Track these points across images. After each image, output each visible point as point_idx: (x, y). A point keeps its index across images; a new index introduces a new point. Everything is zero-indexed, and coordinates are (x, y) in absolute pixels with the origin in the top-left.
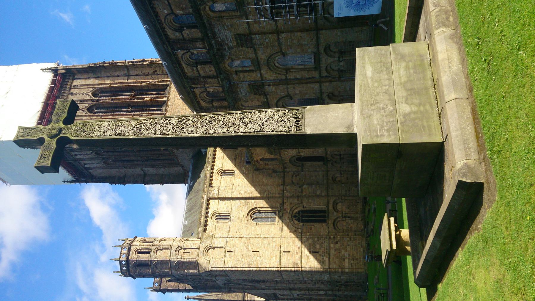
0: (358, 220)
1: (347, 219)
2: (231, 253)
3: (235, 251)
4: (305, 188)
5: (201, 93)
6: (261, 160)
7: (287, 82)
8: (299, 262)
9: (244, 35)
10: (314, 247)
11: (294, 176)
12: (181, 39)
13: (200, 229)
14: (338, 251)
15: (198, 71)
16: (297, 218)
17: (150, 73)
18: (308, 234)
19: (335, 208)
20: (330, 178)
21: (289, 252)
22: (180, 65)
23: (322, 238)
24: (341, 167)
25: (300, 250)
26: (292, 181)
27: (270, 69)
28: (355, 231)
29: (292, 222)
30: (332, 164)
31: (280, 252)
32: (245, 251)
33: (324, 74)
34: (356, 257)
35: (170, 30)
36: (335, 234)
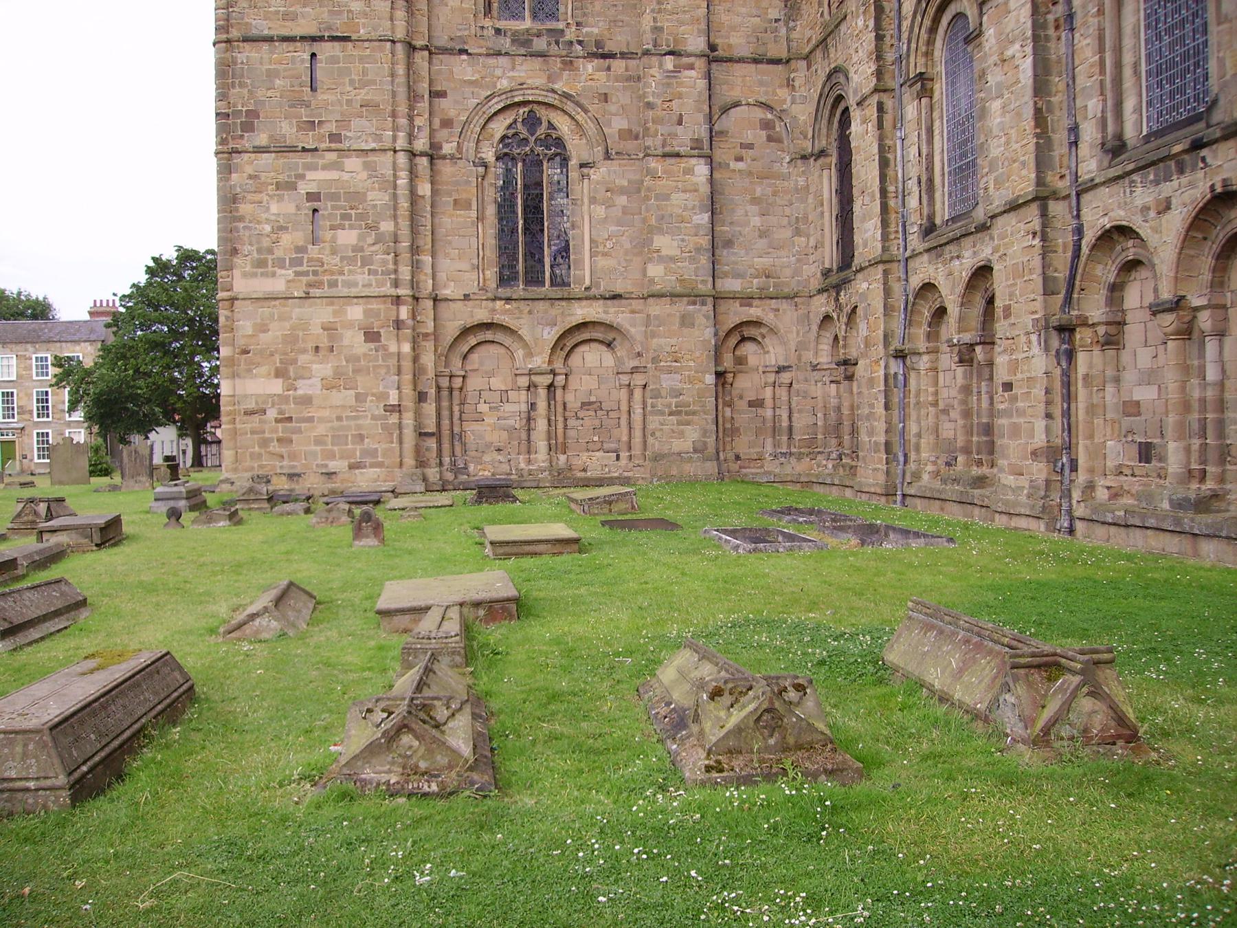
4: (689, 171)
8: (262, 139)
11: (769, 116)
16: (524, 133)
19: (586, 336)
20: (754, 312)
21: (313, 89)
23: (396, 263)
24: (815, 368)
25: (323, 146)
26: (737, 104)
28: (457, 437)
30: (827, 318)
31: (314, 39)
34: (294, 437)
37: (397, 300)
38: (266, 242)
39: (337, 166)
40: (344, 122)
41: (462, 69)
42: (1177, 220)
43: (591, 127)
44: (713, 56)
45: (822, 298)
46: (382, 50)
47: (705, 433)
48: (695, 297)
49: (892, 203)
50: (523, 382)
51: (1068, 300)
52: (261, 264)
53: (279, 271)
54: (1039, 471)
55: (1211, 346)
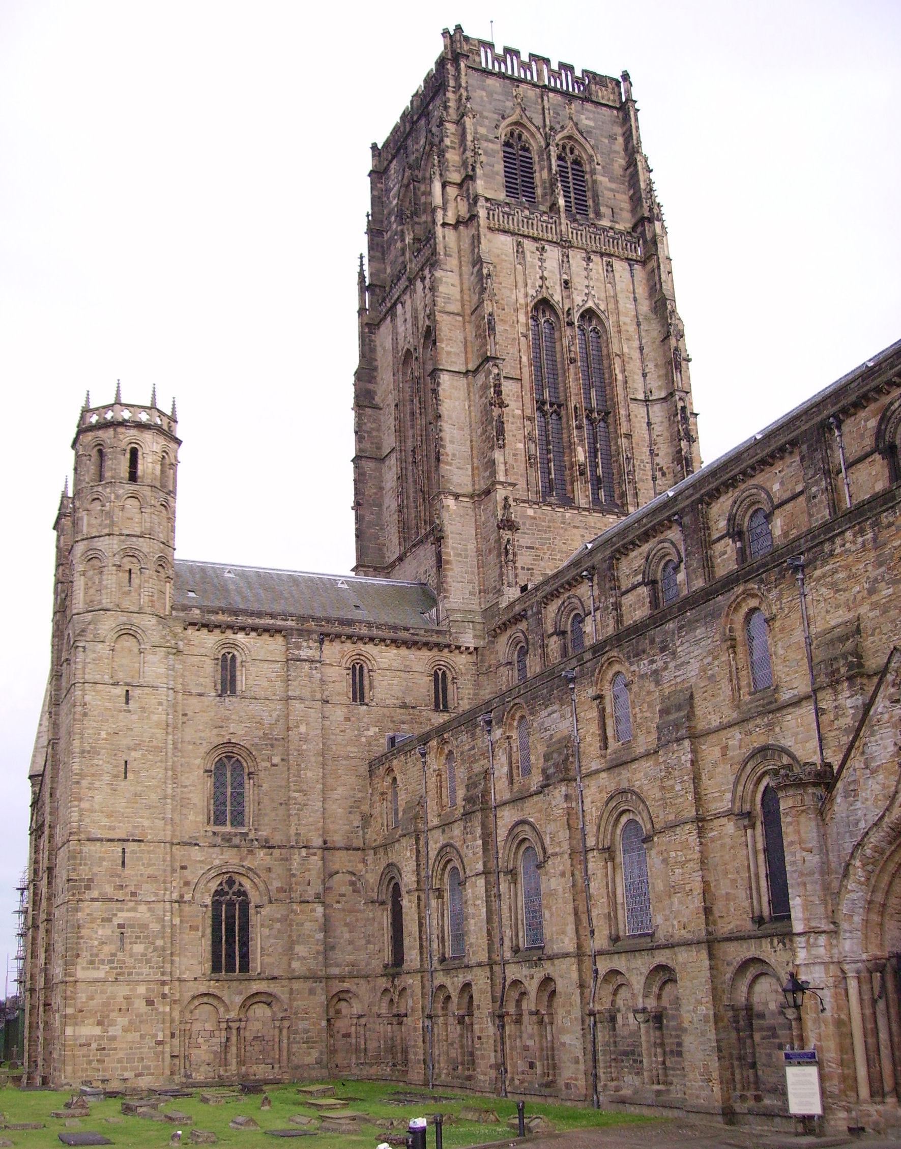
2: (124, 700)
3: (130, 711)
4: (313, 910)
5: (580, 600)
6: (395, 779)
7: (579, 854)
8: (95, 894)
9: (691, 716)
10: (138, 937)
12: (709, 535)
13: (197, 611)
14: (124, 1007)
15: (634, 587)
16: (226, 889)
17: (657, 460)
18: (177, 921)
19: (257, 999)
20: (346, 985)
22: (646, 536)
23: (163, 962)
24: (379, 1016)
25: (129, 898)
26: (337, 873)
27: (611, 798)
29: (213, 873)
30: (386, 990)
31: (124, 840)
32: (127, 742)
33: (604, 966)
35: (730, 502)
36: (177, 997)
37: (163, 983)
38: (95, 951)
39: (134, 909)
40: (138, 886)
41: (196, 854)
42: (535, 983)
43: (262, 886)
44: (327, 847)
45: (384, 979)
46: (159, 847)
47: (321, 1053)
48: (316, 978)
49: (424, 944)
50: (223, 1026)
51: (501, 1005)
52: (92, 962)
53: (102, 967)
54: (493, 1073)
55: (548, 1028)
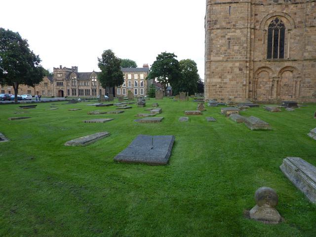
0: (269, 95)
1: (271, 83)
8: (218, 26)
14: (230, 71)
18: (253, 37)
23: (247, 53)
25: (232, 27)
28: (255, 92)
29: (269, 17)
36: (252, 67)
37: (247, 62)
38: (218, 49)
39: (234, 32)
40: (236, 22)
41: (261, 8)
50: (271, 80)
52: (217, 54)
